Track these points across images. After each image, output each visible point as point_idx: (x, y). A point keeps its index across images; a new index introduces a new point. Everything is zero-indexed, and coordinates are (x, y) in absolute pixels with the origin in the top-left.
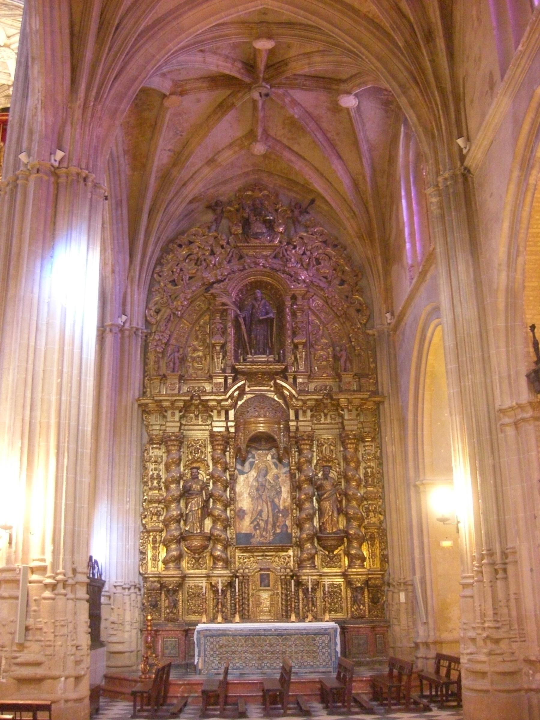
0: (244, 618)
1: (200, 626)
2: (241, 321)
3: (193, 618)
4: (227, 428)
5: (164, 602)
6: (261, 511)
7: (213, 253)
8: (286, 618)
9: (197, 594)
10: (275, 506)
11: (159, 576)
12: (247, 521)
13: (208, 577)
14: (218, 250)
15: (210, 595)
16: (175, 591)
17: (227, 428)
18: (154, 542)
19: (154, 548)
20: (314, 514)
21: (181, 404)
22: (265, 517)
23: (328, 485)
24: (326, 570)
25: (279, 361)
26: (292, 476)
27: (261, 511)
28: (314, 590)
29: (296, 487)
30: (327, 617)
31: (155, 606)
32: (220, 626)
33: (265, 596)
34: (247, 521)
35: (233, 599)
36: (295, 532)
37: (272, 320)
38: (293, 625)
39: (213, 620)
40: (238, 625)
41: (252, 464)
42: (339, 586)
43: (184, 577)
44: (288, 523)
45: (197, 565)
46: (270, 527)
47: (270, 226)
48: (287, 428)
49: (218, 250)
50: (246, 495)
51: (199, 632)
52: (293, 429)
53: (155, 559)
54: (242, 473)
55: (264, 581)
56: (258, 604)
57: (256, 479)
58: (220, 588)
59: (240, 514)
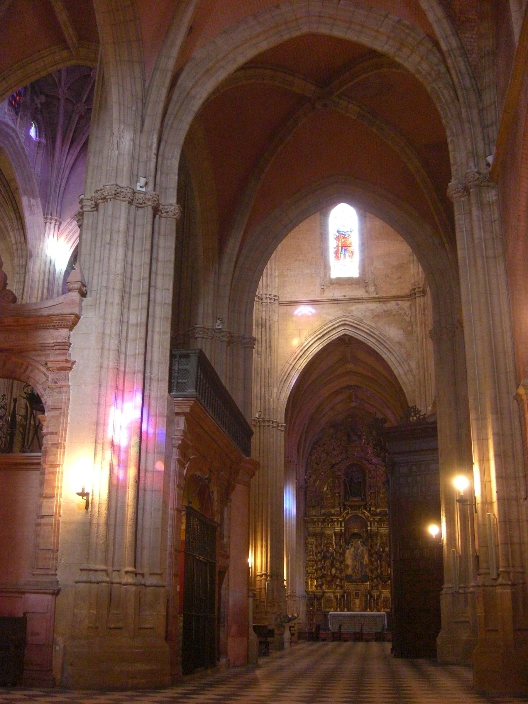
0: (348, 611)
1: (331, 613)
2: (347, 482)
3: (327, 610)
4: (341, 530)
5: (316, 603)
6: (356, 566)
7: (334, 449)
8: (366, 611)
9: (329, 600)
10: (362, 563)
11: (314, 593)
12: (350, 569)
13: (334, 593)
14: (337, 448)
15: (334, 600)
16: (320, 599)
17: (341, 530)
18: (311, 578)
19: (311, 581)
20: (378, 567)
21: (322, 520)
22: (357, 567)
23: (384, 555)
24: (383, 591)
25: (362, 500)
26: (369, 551)
27: (356, 566)
28: (377, 599)
29: (370, 555)
30: (382, 610)
31: (312, 605)
32: (339, 613)
33: (357, 601)
34: (350, 569)
35: (344, 602)
36: (370, 574)
37: (360, 482)
38: (368, 613)
39: (336, 610)
40: (346, 613)
41: (352, 545)
42: (389, 597)
43: (324, 593)
44: (367, 570)
45: (329, 588)
46: (359, 572)
47: (360, 437)
48: (367, 530)
49: (337, 448)
50: (349, 558)
51: (330, 615)
52: (369, 531)
53: (312, 585)
54: (348, 549)
55: (357, 595)
56: (354, 604)
57: (354, 551)
58: (339, 597)
59: (347, 566)
